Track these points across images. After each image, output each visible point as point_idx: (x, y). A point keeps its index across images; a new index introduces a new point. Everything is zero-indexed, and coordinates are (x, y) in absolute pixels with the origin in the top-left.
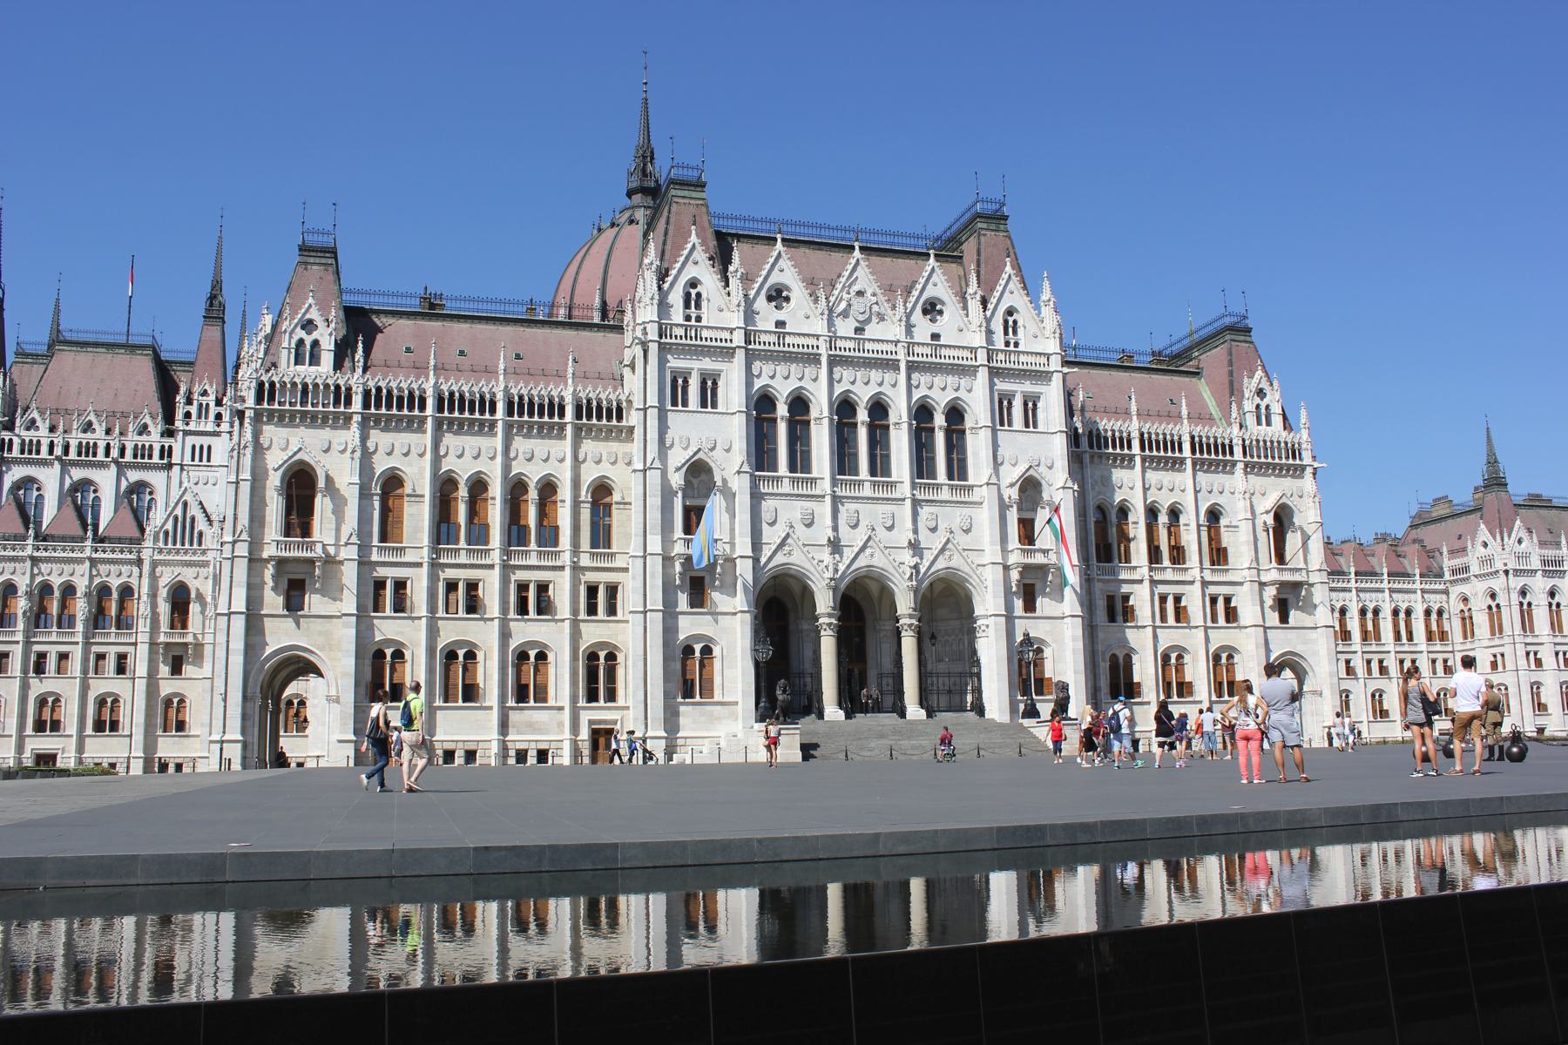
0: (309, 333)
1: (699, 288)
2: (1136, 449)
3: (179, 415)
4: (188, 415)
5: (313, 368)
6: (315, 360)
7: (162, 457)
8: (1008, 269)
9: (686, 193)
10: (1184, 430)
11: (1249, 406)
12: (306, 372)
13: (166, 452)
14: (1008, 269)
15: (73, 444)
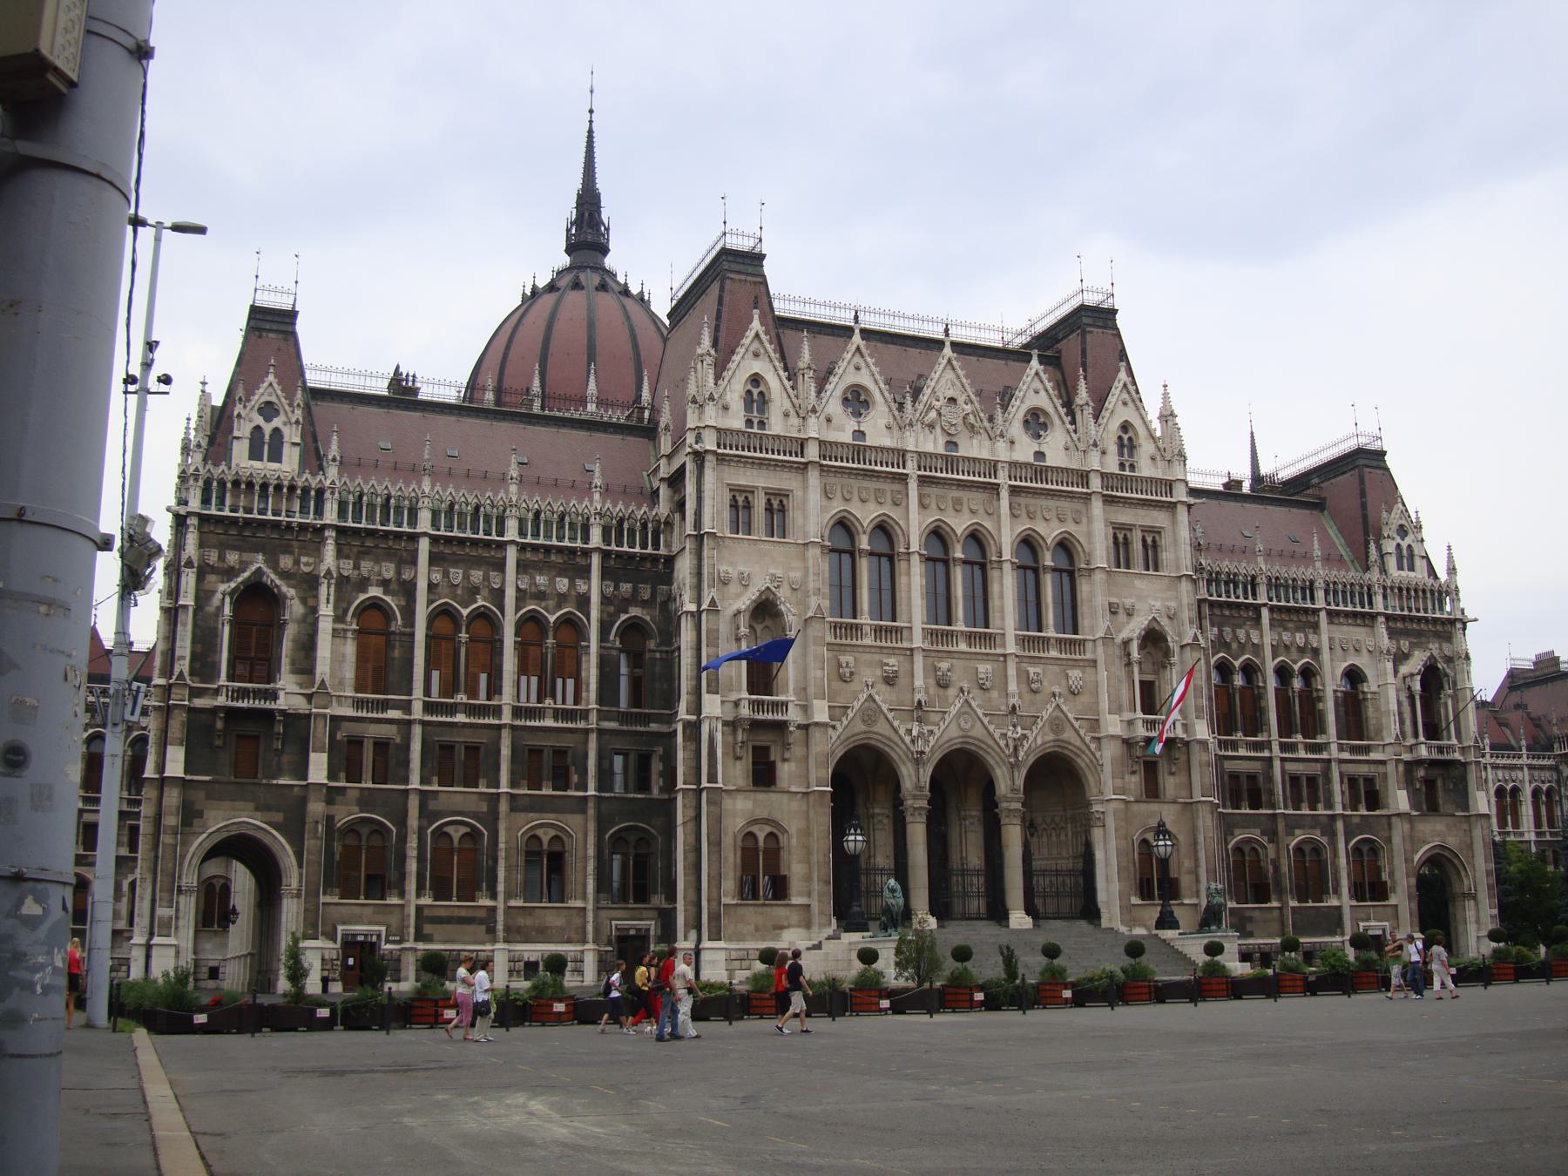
0: (268, 420)
1: (762, 388)
5: (275, 466)
6: (276, 456)
9: (741, 267)
11: (1389, 547)
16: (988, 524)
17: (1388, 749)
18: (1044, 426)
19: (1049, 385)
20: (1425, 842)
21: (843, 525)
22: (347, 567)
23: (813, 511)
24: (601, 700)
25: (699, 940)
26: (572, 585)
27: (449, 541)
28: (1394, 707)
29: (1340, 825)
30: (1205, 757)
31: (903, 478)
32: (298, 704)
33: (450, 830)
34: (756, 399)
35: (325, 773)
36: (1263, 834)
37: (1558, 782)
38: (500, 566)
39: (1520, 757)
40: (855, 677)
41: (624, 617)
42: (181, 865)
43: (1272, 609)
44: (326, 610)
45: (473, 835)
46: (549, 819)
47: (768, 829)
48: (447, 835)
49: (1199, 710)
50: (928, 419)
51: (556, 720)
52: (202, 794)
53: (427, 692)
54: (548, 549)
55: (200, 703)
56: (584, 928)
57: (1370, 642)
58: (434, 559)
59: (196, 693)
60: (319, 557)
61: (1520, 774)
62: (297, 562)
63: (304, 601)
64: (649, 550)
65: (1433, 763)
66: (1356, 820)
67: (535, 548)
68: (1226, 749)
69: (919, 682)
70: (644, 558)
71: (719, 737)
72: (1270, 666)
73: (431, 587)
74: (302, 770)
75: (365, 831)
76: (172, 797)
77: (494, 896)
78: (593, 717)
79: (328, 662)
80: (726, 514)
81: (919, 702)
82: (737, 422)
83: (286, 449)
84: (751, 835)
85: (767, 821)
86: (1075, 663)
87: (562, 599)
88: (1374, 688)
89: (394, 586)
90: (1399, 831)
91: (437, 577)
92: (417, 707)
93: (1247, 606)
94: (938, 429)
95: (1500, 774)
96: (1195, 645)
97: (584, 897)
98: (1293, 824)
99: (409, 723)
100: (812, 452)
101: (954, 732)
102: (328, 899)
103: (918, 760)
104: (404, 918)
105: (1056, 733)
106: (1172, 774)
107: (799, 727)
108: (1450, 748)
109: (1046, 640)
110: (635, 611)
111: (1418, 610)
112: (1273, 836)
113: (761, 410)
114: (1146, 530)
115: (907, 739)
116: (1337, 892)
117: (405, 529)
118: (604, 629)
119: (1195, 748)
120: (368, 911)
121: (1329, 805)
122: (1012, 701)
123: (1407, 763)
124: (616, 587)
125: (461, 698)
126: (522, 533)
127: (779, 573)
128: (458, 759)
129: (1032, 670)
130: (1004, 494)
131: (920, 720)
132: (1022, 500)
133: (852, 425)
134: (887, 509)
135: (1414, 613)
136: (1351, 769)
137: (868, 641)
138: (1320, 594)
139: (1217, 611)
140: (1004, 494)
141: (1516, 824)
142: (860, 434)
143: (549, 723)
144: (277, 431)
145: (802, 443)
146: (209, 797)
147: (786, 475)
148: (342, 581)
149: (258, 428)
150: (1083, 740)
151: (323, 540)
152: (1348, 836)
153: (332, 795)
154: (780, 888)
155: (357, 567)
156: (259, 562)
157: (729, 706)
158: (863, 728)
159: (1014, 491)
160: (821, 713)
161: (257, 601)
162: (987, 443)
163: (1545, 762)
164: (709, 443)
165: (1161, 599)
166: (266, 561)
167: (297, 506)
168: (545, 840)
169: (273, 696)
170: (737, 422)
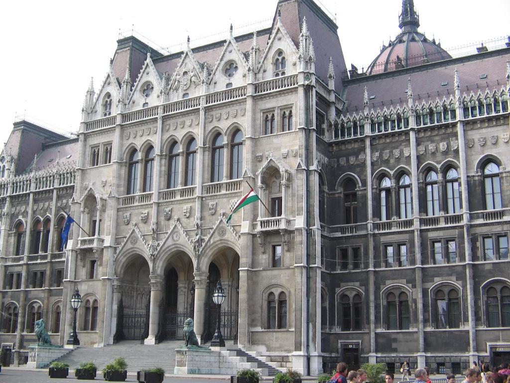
2: (412, 124)
5: (3, 179)
36: (408, 282)
40: (131, 223)
45: (40, 307)
50: (174, 88)
66: (487, 267)
68: (384, 228)
73: (34, 212)
81: (153, 229)
92: (25, 258)
93: (400, 134)
98: (427, 275)
101: (170, 242)
109: (220, 186)
112: (412, 282)
114: (282, 108)
116: (466, 320)
120: (10, 337)
128: (36, 279)
132: (213, 113)
134: (149, 138)
136: (485, 230)
137: (136, 204)
144: (4, 166)
160: (108, 241)
165: (288, 148)
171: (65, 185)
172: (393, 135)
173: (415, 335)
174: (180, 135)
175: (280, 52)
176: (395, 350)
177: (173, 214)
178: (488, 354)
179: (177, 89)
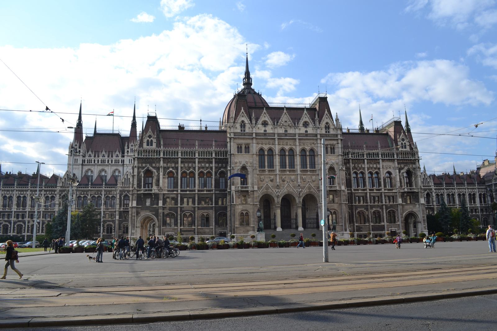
0: (150, 138)
2: (365, 157)
3: (126, 151)
4: (128, 151)
6: (152, 145)
7: (122, 163)
8: (326, 112)
10: (380, 151)
11: (399, 143)
12: (149, 147)
13: (123, 161)
14: (326, 112)
15: (100, 160)
16: (294, 147)
17: (397, 189)
18: (308, 125)
19: (308, 116)
20: (407, 210)
21: (262, 150)
22: (165, 165)
23: (255, 148)
24: (215, 187)
25: (231, 234)
26: (209, 165)
27: (184, 158)
28: (398, 180)
29: (384, 207)
30: (344, 194)
31: (274, 139)
32: (157, 191)
33: (186, 214)
34: (243, 125)
35: (162, 204)
37: (487, 192)
38: (195, 163)
39: (465, 186)
41: (220, 171)
42: (136, 222)
43: (367, 160)
44: (161, 174)
46: (206, 211)
47: (246, 212)
48: (186, 215)
49: (343, 184)
51: (207, 191)
52: (140, 209)
53: (181, 187)
54: (204, 159)
55: (139, 192)
56: (213, 232)
57: (393, 166)
58: (182, 162)
59: (138, 191)
60: (159, 163)
61: (475, 190)
62: (156, 165)
63: (157, 172)
64: (225, 157)
65: (408, 192)
66: (389, 206)
67: (201, 158)
68: (356, 191)
69: (278, 180)
70: (223, 159)
71: (234, 194)
72: (367, 172)
73: (181, 167)
74: (158, 204)
75: (170, 215)
76: (134, 210)
77: (195, 226)
78: (214, 191)
79: (162, 183)
80: (236, 150)
82: (239, 130)
83: (153, 143)
84: (242, 213)
85: (246, 210)
86: (314, 175)
87: (207, 168)
88: (394, 176)
89: (174, 168)
90: (400, 208)
91: (182, 166)
94: (283, 128)
95: (470, 190)
96: (342, 170)
97: (213, 226)
98: (372, 207)
99: (178, 194)
100: (254, 135)
101: (286, 190)
102: (163, 228)
103: (278, 197)
104: (178, 231)
105: (309, 190)
106: (337, 197)
107: (251, 191)
108: (414, 189)
110: (222, 169)
111: (406, 158)
112: (367, 210)
113: (244, 128)
115: (275, 193)
116: (383, 221)
117: (176, 157)
118: (216, 173)
119: (342, 191)
121: (382, 202)
122: (299, 184)
123: (402, 192)
124: (218, 165)
125: (188, 189)
126: (199, 156)
127: (247, 160)
129: (304, 177)
130: (297, 140)
131: (278, 189)
132: (302, 141)
133: (264, 129)
134: (271, 146)
135: (405, 158)
136: (388, 194)
137: (267, 173)
138: (380, 156)
139: (354, 161)
140: (297, 140)
141: (475, 202)
142: (265, 131)
143: (205, 192)
144: (152, 140)
145: (252, 133)
146: (141, 210)
147: (249, 140)
148: (164, 168)
149: (148, 140)
150: (315, 191)
151: (160, 160)
152: (386, 209)
153: (164, 208)
154: (248, 224)
155: (167, 165)
156: (148, 165)
157: (237, 188)
158: (266, 191)
159: (299, 139)
160: (256, 188)
161: (148, 173)
162: (294, 130)
163: (483, 187)
164: (232, 136)
166: (149, 165)
167: (155, 154)
168: (205, 215)
169: (151, 190)
170: (239, 130)
171: (203, 157)
172: (359, 159)
173: (368, 226)
174: (287, 148)
175: (327, 123)
176: (362, 231)
177: (286, 179)
178: (390, 232)
179: (281, 127)
